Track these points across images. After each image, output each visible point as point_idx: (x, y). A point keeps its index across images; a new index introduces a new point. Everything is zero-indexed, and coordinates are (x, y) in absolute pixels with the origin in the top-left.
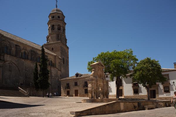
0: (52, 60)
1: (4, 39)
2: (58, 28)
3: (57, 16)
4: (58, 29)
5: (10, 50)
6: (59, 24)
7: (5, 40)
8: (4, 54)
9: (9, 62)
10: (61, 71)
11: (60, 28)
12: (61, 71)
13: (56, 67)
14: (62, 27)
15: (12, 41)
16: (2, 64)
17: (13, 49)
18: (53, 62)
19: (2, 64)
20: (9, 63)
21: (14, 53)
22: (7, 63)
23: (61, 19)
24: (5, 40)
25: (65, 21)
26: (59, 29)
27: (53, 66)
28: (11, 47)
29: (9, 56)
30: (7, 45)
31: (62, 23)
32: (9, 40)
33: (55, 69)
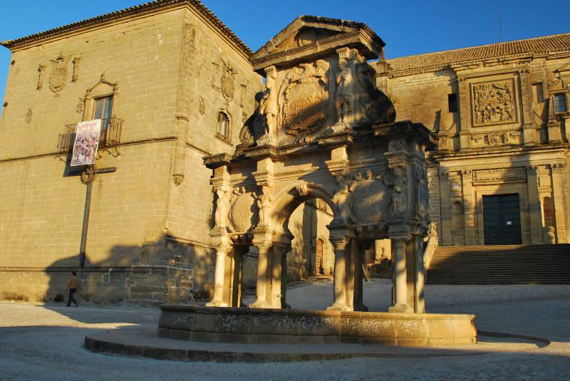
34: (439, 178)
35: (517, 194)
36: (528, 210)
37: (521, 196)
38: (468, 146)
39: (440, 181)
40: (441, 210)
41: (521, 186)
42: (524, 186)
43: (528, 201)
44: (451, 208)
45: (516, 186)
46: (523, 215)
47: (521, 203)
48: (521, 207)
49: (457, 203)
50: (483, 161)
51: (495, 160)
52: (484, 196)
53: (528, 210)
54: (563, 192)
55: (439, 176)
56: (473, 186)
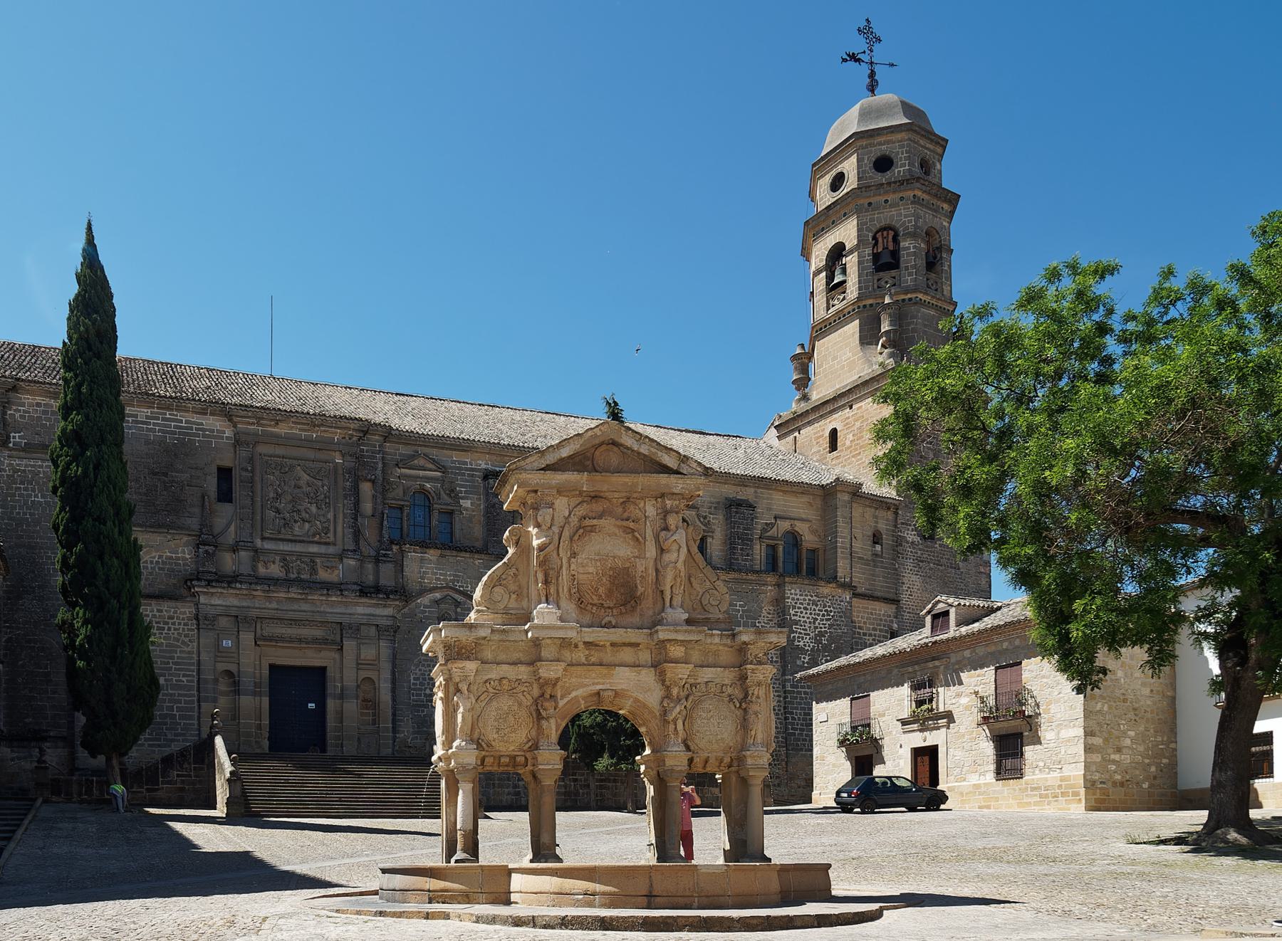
0: (801, 528)
1: (404, 450)
5: (451, 513)
7: (413, 457)
8: (402, 552)
9: (438, 595)
10: (895, 601)
11: (895, 254)
12: (895, 601)
13: (833, 579)
14: (914, 235)
15: (456, 456)
16: (389, 611)
17: (466, 503)
18: (809, 539)
19: (389, 611)
20: (437, 602)
21: (478, 531)
22: (425, 600)
24: (413, 457)
26: (886, 259)
27: (813, 573)
28: (453, 493)
29: (432, 555)
31: (916, 201)
32: (434, 453)
33: (826, 590)
34: (198, 625)
35: (323, 670)
36: (342, 697)
37: (330, 673)
39: (198, 629)
44: (216, 681)
46: (331, 704)
47: (329, 685)
48: (330, 691)
49: (229, 674)
52: (272, 667)
54: (393, 673)
55: (197, 619)
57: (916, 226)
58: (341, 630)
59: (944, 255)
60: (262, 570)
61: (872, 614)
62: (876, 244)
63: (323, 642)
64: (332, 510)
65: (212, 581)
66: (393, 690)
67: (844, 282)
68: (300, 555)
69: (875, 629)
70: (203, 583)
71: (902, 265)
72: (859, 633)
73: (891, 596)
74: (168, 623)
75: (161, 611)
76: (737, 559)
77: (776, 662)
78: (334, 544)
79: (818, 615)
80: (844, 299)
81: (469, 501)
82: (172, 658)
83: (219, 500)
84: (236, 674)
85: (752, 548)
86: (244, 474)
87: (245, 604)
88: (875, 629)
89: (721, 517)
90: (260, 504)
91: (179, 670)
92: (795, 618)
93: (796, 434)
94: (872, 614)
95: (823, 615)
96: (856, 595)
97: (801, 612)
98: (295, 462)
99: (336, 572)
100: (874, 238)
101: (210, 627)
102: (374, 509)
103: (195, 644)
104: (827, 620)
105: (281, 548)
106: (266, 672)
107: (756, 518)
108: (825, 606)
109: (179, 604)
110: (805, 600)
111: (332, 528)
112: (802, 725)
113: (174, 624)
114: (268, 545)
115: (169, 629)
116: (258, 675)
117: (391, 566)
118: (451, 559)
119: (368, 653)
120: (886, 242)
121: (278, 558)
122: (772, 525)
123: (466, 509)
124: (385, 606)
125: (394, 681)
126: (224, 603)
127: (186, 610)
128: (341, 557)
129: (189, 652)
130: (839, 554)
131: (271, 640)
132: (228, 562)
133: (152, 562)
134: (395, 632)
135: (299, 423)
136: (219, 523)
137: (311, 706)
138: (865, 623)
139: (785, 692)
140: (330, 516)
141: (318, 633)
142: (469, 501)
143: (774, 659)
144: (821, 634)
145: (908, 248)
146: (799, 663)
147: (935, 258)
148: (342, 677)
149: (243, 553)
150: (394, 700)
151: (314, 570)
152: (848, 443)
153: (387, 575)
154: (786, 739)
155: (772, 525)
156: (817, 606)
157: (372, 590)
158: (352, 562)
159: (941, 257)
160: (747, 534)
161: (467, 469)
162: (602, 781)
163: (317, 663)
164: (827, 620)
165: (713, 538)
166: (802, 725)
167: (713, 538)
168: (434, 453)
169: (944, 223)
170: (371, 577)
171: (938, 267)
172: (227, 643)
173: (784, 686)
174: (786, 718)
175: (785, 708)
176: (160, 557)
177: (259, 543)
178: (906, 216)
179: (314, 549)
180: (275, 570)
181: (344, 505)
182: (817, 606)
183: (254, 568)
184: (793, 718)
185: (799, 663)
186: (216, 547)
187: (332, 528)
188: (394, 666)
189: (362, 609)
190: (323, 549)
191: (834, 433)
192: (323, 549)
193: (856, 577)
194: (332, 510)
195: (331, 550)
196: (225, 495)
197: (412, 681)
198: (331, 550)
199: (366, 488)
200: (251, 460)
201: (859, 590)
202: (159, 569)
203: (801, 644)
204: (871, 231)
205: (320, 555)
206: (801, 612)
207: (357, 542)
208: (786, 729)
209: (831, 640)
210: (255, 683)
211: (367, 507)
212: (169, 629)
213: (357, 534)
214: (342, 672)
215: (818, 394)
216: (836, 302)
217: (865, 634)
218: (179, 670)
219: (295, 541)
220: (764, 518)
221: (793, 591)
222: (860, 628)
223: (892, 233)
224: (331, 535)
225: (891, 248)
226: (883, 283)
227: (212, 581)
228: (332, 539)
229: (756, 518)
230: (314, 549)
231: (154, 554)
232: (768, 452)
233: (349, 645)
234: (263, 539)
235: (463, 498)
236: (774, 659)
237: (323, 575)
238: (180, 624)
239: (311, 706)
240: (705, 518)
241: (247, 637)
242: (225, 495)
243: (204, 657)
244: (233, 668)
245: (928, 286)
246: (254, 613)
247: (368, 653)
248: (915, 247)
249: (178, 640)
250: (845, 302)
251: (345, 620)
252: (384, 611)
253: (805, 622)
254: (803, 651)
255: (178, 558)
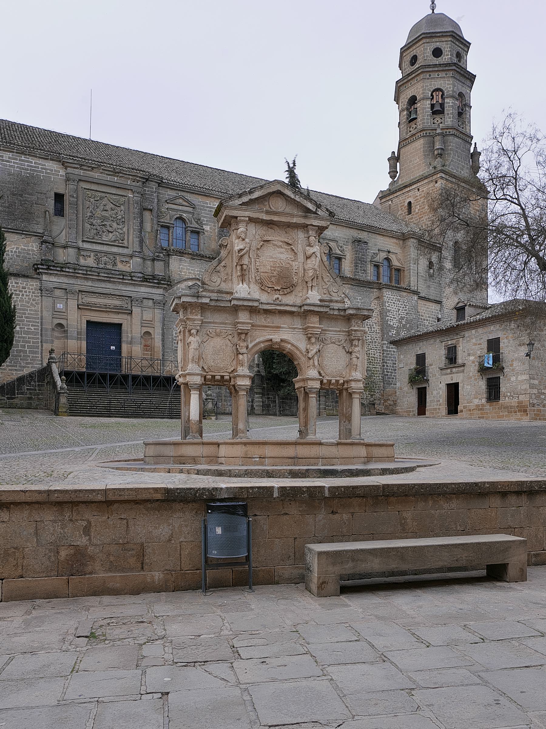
2: (433, 106)
3: (429, 52)
4: (435, 113)
6: (437, 84)
9: (190, 283)
11: (442, 105)
17: (207, 228)
22: (183, 285)
23: (446, 58)
24: (176, 198)
25: (470, 68)
26: (437, 108)
28: (198, 221)
30: (185, 215)
36: (131, 343)
37: (124, 328)
38: (76, 262)
40: (42, 331)
41: (125, 316)
42: (129, 317)
43: (132, 333)
45: (120, 316)
47: (124, 335)
48: (124, 339)
49: (60, 325)
50: (90, 283)
51: (103, 285)
52: (88, 322)
53: (131, 343)
54: (163, 329)
55: (41, 290)
56: (78, 308)
57: (453, 91)
58: (131, 301)
59: (467, 109)
60: (82, 262)
61: (428, 308)
62: (433, 98)
63: (118, 310)
64: (126, 226)
65: (51, 266)
66: (163, 340)
67: (416, 118)
68: (106, 253)
69: (429, 317)
70: (45, 267)
71: (446, 112)
72: (421, 319)
73: (438, 299)
74: (22, 291)
75: (18, 283)
76: (358, 272)
77: (379, 333)
78: (128, 248)
79: (401, 307)
80: (416, 128)
81: (209, 227)
82: (25, 314)
83: (56, 215)
84: (66, 326)
85: (366, 266)
86: (72, 199)
87: (71, 282)
88: (429, 317)
89: (350, 247)
90: (81, 219)
91: (29, 321)
92: (388, 308)
93: (390, 202)
94: (428, 308)
95: (403, 308)
96: (421, 298)
97: (392, 305)
98: (104, 195)
99: (128, 265)
100: (432, 95)
101: (49, 295)
102: (152, 227)
103: (40, 306)
104: (405, 310)
105: (95, 248)
106: (84, 326)
107: (368, 249)
108: (404, 302)
109: (29, 280)
110: (394, 298)
111: (126, 237)
112: (392, 370)
113: (26, 292)
114: (86, 246)
115: (23, 295)
116: (79, 327)
117: (162, 263)
118: (198, 261)
119: (148, 316)
120: (438, 97)
121: (92, 254)
122: (377, 254)
123: (207, 231)
124: (158, 287)
125: (163, 335)
126: (58, 281)
127: (33, 284)
128: (131, 257)
129: (36, 311)
130: (411, 273)
131: (88, 306)
132: (62, 256)
133: (12, 252)
134: (164, 304)
135: (106, 170)
136: (56, 230)
137: (113, 348)
138: (424, 313)
139: (383, 351)
140: (125, 229)
141: (117, 302)
142: (209, 227)
143: (378, 331)
144: (402, 318)
145: (449, 103)
146: (390, 334)
147: (462, 110)
148: (132, 331)
149: (70, 250)
150: (163, 346)
151: (115, 264)
152: (417, 210)
153: (159, 269)
154: (383, 377)
155: (377, 254)
156: (400, 302)
157: (151, 277)
158: (138, 260)
159: (466, 110)
160: (364, 258)
161: (208, 207)
162: (283, 399)
163: (116, 321)
164: (405, 310)
165: (345, 259)
166: (392, 370)
167: (345, 259)
168: (188, 196)
169: (468, 91)
170: (150, 269)
171: (464, 116)
172: (60, 306)
173: (382, 347)
174: (383, 366)
175: (383, 360)
176: (17, 248)
177: (80, 244)
178: (448, 84)
179: (115, 250)
180: (90, 262)
181: (134, 223)
182: (400, 302)
183: (78, 259)
184: (387, 366)
185: (390, 334)
186: (53, 244)
187: (126, 237)
188: (164, 325)
189: (144, 290)
190: (121, 250)
191: (410, 203)
192: (121, 250)
193: (420, 287)
194: (126, 226)
195: (125, 251)
196: (60, 212)
197: (174, 335)
198: (125, 251)
199: (147, 214)
200: (76, 191)
201: (421, 295)
202: (17, 256)
203: (392, 323)
204: (430, 90)
205: (120, 254)
206: (392, 305)
207: (142, 248)
208: (384, 371)
209: (407, 322)
210: (78, 332)
211: (148, 226)
212: (23, 295)
213: (141, 242)
214: (131, 327)
215: (401, 181)
216: (411, 129)
217: (424, 320)
218: (29, 321)
219: (103, 244)
220: (372, 250)
221: (387, 293)
222: (422, 316)
223: (441, 93)
224: (125, 242)
225: (440, 102)
226: (436, 122)
227: (51, 266)
228: (126, 245)
229: (368, 249)
230: (115, 250)
231: (13, 246)
232: (376, 212)
233: (136, 310)
234: (83, 241)
235: (205, 224)
236: (378, 331)
237: (120, 267)
238: (29, 292)
239: (113, 348)
240: (341, 247)
241: (73, 304)
242: (60, 212)
243: (45, 314)
244: (63, 322)
245: (459, 126)
246: (77, 288)
247: (148, 316)
248: (452, 103)
249: (28, 303)
250: (416, 130)
251: (133, 295)
252: (157, 293)
253: (394, 311)
254: (392, 327)
255: (29, 250)
